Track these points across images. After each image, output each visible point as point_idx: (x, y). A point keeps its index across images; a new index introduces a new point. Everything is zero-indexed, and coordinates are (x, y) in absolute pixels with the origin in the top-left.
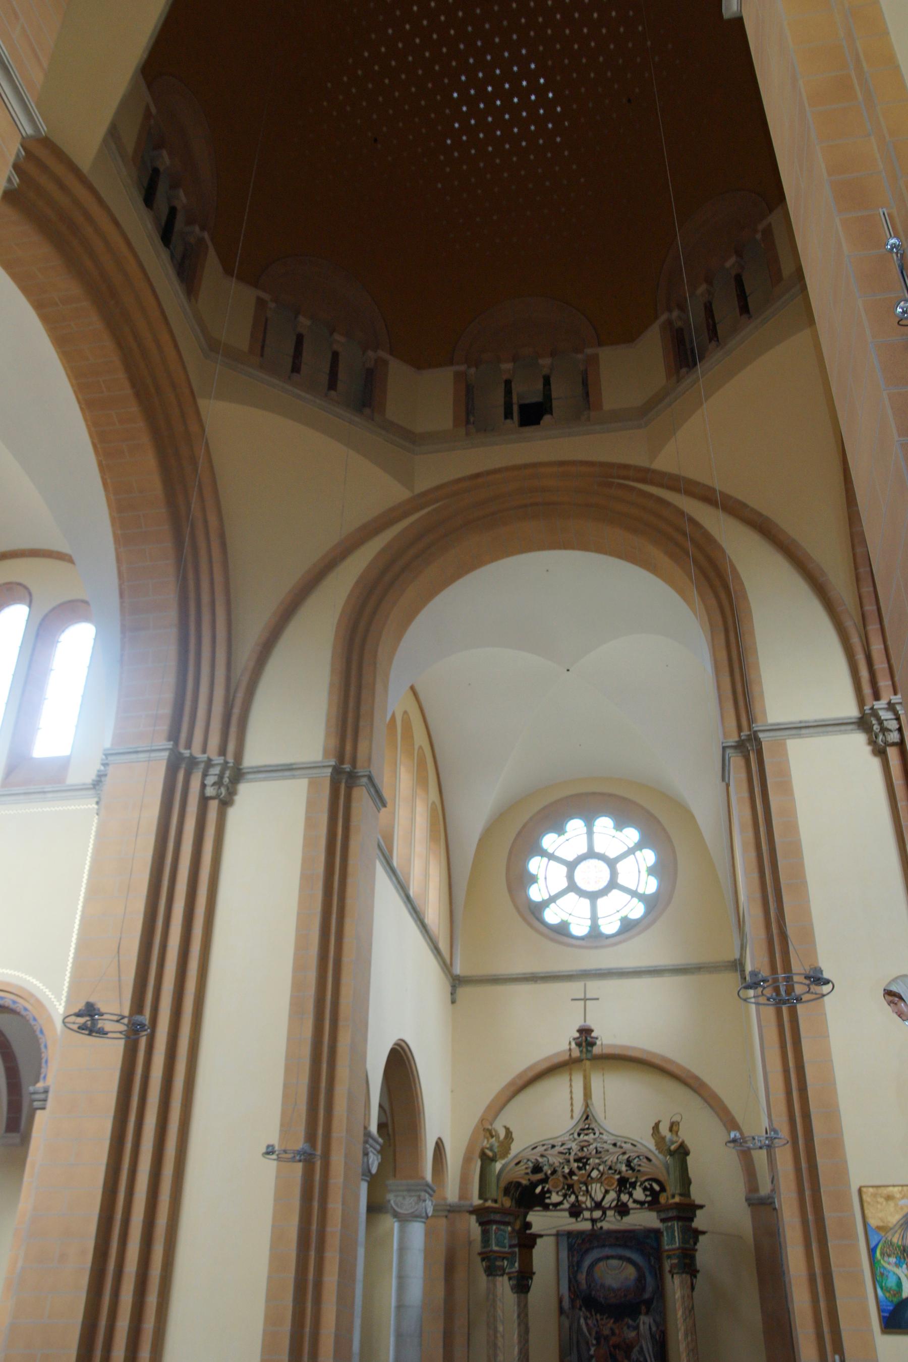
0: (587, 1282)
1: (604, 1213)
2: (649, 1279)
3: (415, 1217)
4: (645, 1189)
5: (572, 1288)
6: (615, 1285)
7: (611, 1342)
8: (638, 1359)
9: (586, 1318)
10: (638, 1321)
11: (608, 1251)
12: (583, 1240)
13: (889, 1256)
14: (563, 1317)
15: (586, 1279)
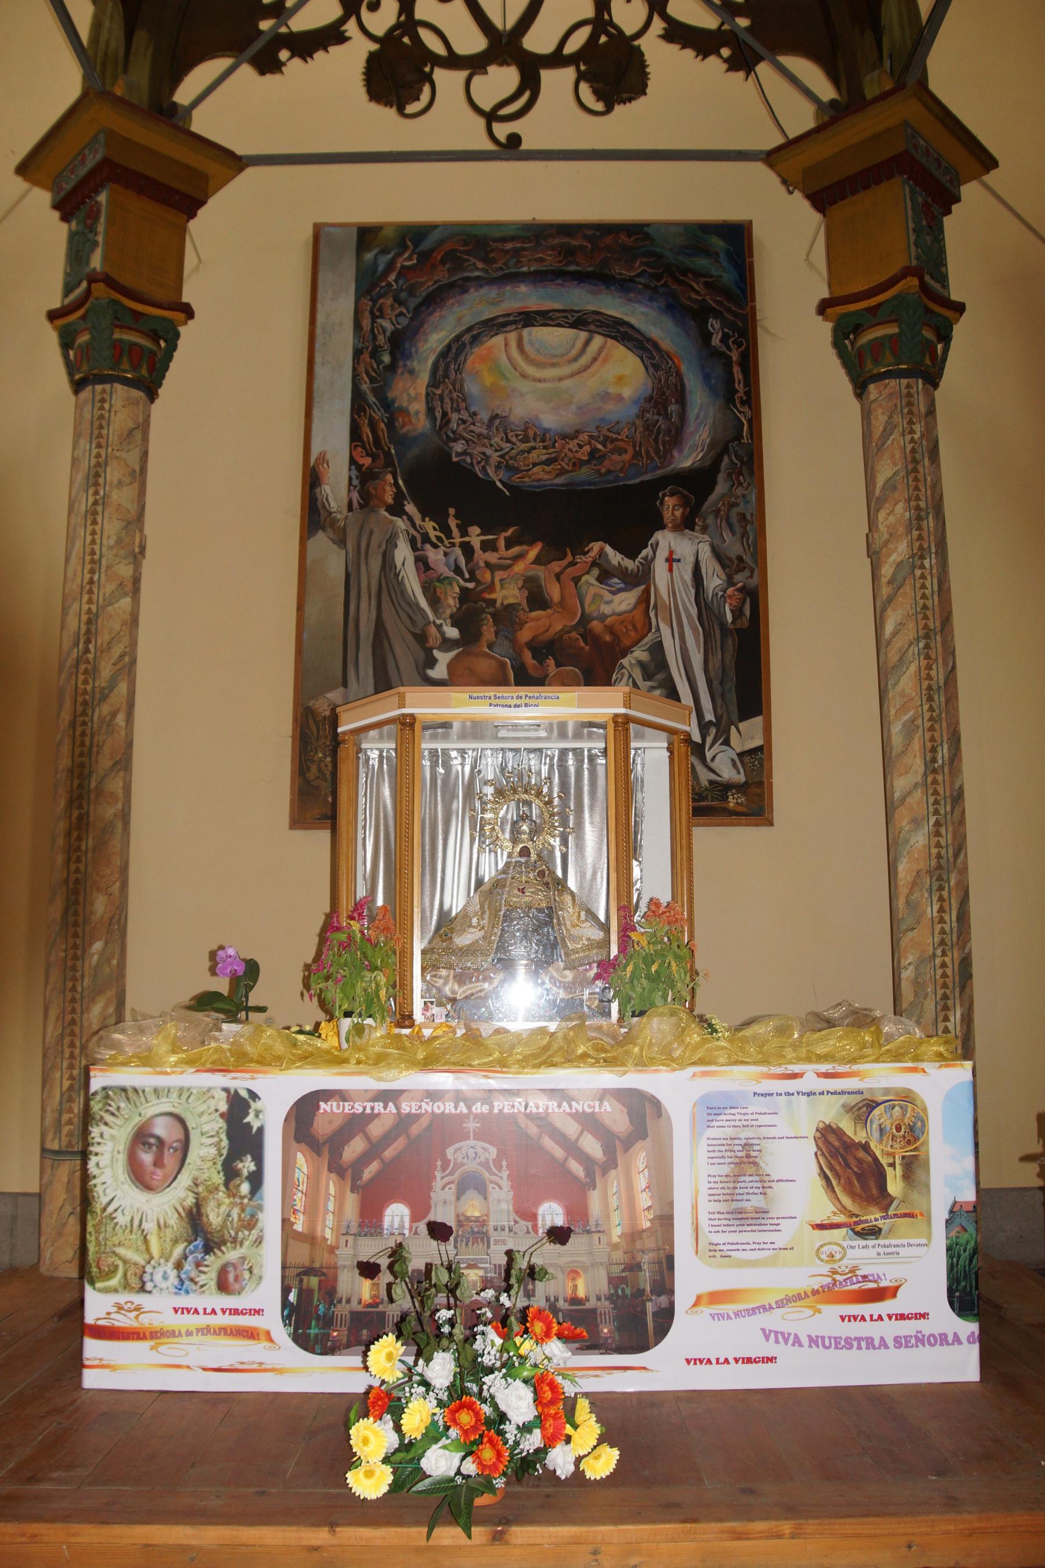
0: (430, 411)
1: (530, 84)
5: (366, 430)
6: (550, 420)
7: (525, 635)
10: (647, 552)
12: (425, 257)
14: (321, 541)
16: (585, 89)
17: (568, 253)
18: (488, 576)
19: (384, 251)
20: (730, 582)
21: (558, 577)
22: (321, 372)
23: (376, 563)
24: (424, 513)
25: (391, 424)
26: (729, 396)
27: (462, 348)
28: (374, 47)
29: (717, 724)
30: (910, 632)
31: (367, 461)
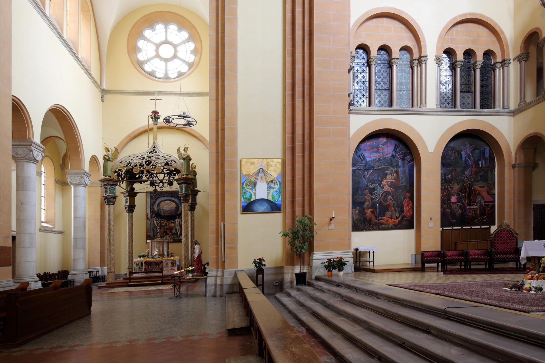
1: (163, 185)
3: (80, 184)
6: (167, 210)
7: (165, 228)
9: (156, 220)
11: (165, 198)
12: (156, 195)
13: (249, 186)
17: (169, 194)
21: (168, 223)
22: (147, 206)
23: (153, 222)
25: (154, 210)
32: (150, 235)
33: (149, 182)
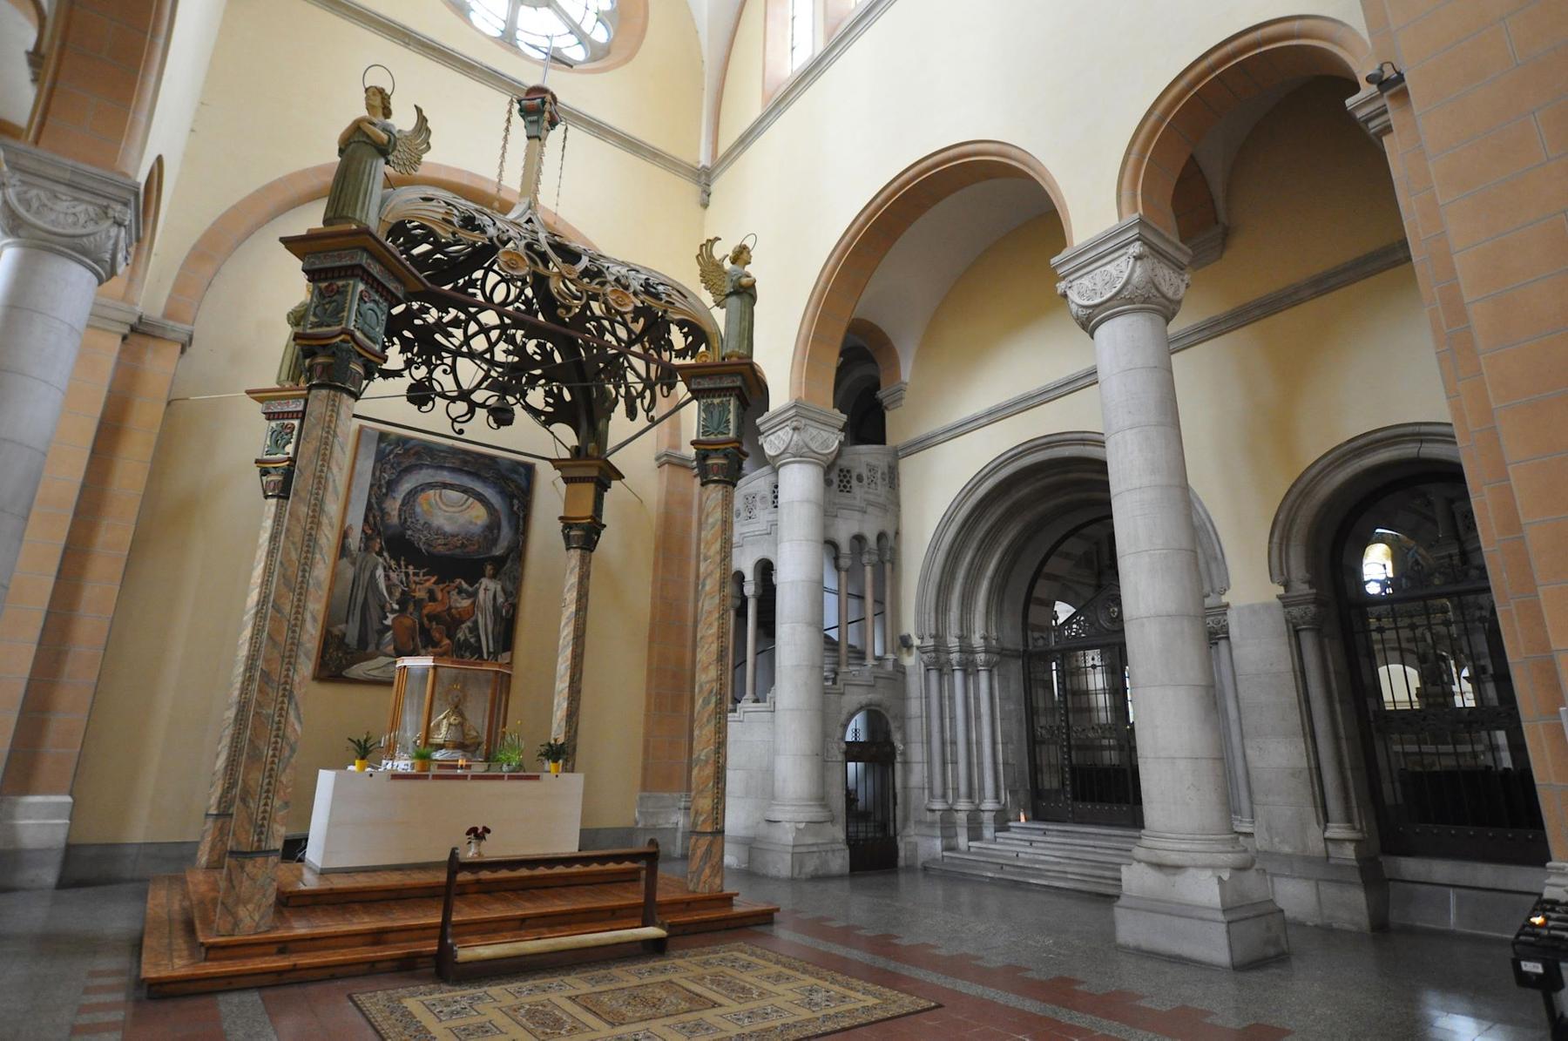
0: (400, 515)
1: (471, 411)
2: (506, 532)
4: (548, 394)
5: (371, 518)
6: (448, 528)
7: (425, 612)
8: (466, 640)
10: (477, 585)
11: (446, 477)
12: (406, 451)
15: (400, 510)
16: (491, 418)
17: (465, 462)
18: (414, 586)
19: (390, 445)
20: (506, 600)
21: (442, 590)
22: (355, 492)
23: (367, 574)
24: (392, 557)
26: (517, 529)
27: (416, 493)
28: (414, 382)
29: (494, 653)
30: (571, 636)
31: (370, 532)
32: (344, 635)
33: (404, 383)
